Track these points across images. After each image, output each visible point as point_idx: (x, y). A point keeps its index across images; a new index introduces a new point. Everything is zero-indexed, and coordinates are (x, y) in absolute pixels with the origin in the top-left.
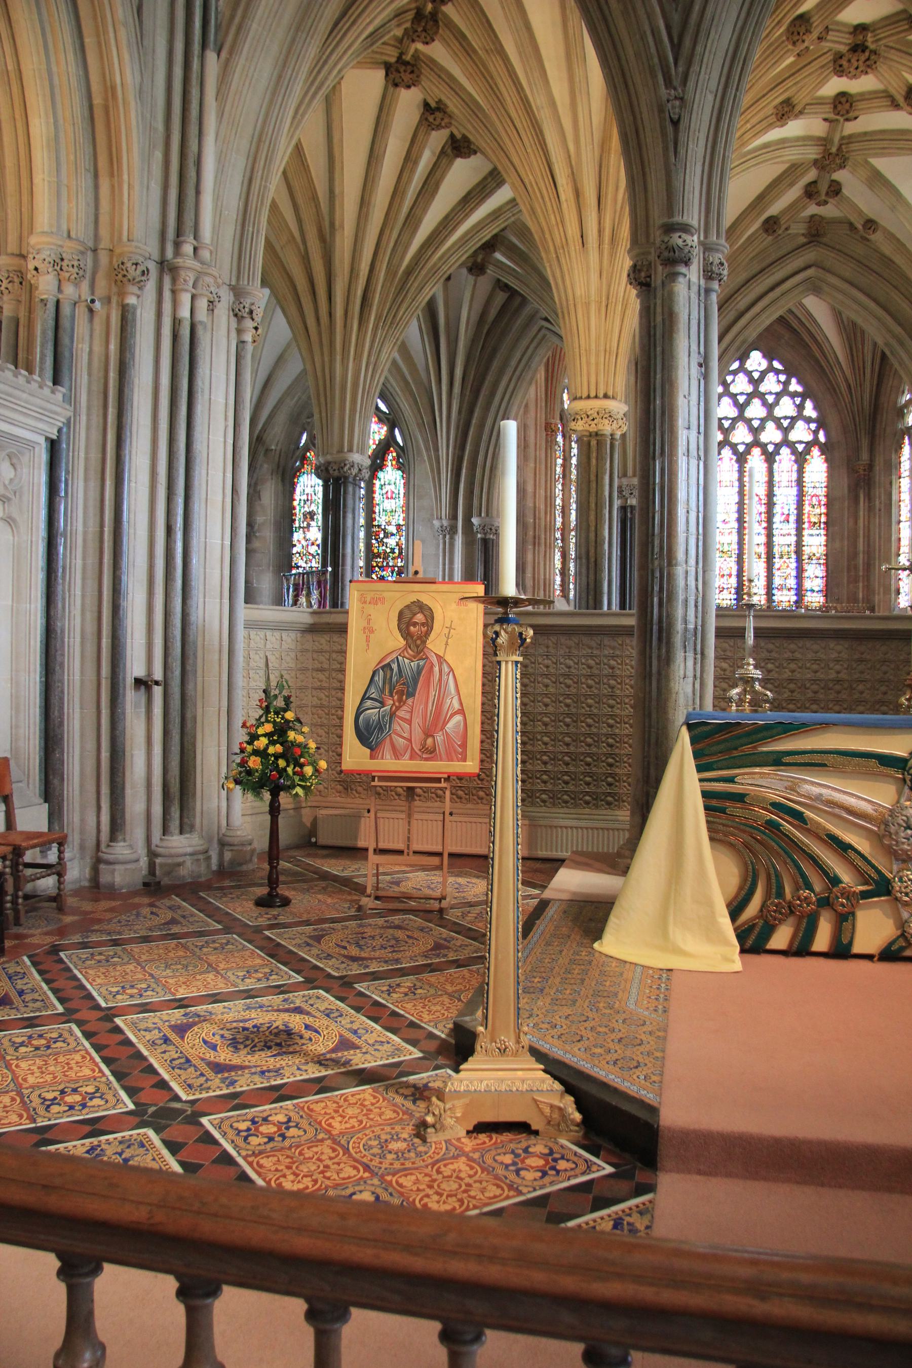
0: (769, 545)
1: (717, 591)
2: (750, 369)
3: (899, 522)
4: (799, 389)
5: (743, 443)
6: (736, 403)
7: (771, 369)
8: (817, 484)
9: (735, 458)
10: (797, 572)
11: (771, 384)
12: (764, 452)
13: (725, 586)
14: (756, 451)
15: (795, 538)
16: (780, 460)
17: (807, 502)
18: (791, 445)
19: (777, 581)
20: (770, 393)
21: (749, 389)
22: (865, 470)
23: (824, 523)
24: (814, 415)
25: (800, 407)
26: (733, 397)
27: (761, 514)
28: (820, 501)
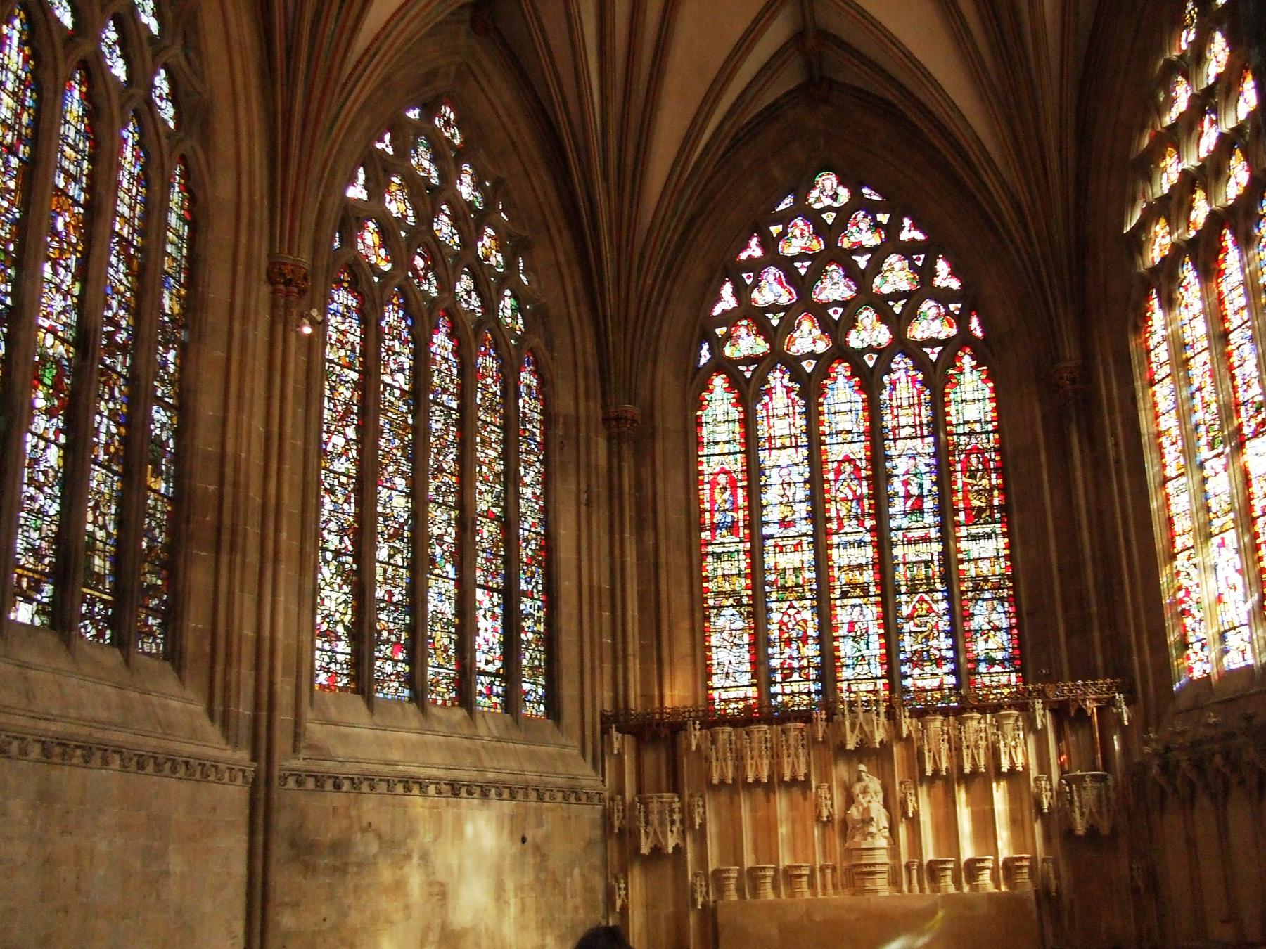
0: (883, 564)
1: (778, 678)
2: (817, 206)
3: (1166, 480)
4: (919, 236)
5: (812, 355)
6: (792, 278)
7: (857, 202)
8: (977, 428)
9: (797, 386)
10: (952, 623)
11: (862, 234)
12: (858, 369)
13: (795, 664)
14: (842, 369)
15: (937, 547)
16: (893, 383)
17: (959, 467)
18: (914, 350)
19: (909, 644)
20: (861, 249)
21: (817, 246)
22: (1073, 381)
23: (1001, 508)
24: (955, 284)
25: (925, 274)
26: (786, 265)
27: (859, 499)
28: (986, 462)
